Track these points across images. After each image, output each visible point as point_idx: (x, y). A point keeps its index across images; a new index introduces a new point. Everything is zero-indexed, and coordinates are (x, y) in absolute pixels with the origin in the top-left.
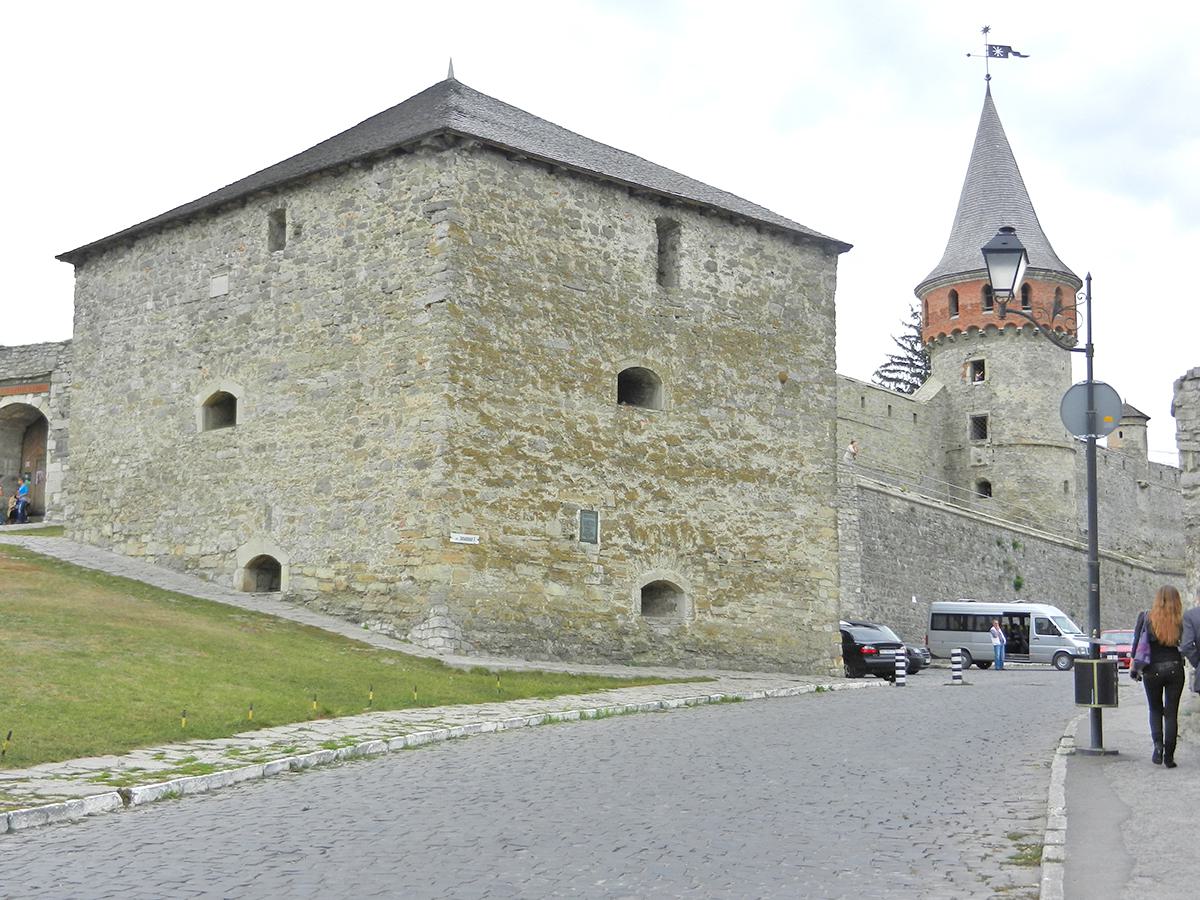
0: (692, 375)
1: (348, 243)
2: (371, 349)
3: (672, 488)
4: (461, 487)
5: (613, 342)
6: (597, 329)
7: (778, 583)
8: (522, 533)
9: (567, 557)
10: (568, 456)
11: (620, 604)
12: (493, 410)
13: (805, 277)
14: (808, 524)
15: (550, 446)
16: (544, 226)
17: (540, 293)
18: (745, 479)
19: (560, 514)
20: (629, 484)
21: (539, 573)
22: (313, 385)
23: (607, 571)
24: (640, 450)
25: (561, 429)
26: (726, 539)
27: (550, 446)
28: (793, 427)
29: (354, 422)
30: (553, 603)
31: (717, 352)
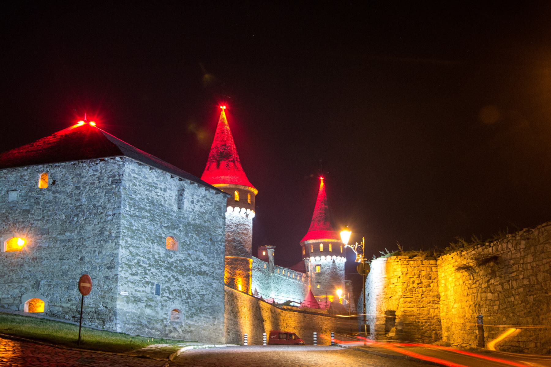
0: (186, 239)
1: (77, 188)
2: (89, 228)
3: (180, 277)
4: (123, 276)
5: (165, 227)
6: (161, 223)
7: (208, 311)
8: (139, 291)
9: (151, 300)
10: (153, 266)
11: (165, 316)
12: (134, 250)
13: (218, 206)
14: (216, 290)
15: (148, 262)
16: (148, 188)
17: (146, 211)
18: (200, 274)
19: (150, 286)
20: (169, 276)
21: (143, 305)
22: (61, 237)
23: (162, 305)
24: (172, 264)
25: (151, 256)
26: (194, 295)
27: (148, 262)
28: (213, 257)
29: (80, 252)
30: (148, 315)
31: (193, 231)
